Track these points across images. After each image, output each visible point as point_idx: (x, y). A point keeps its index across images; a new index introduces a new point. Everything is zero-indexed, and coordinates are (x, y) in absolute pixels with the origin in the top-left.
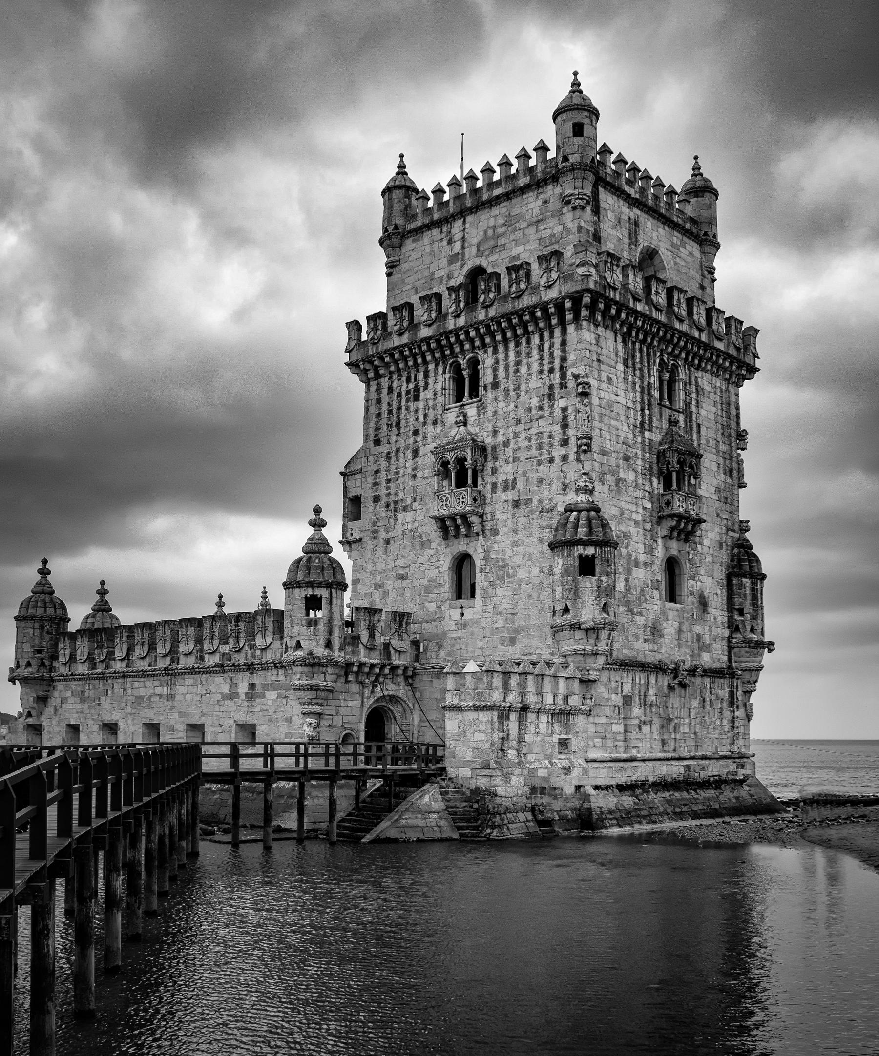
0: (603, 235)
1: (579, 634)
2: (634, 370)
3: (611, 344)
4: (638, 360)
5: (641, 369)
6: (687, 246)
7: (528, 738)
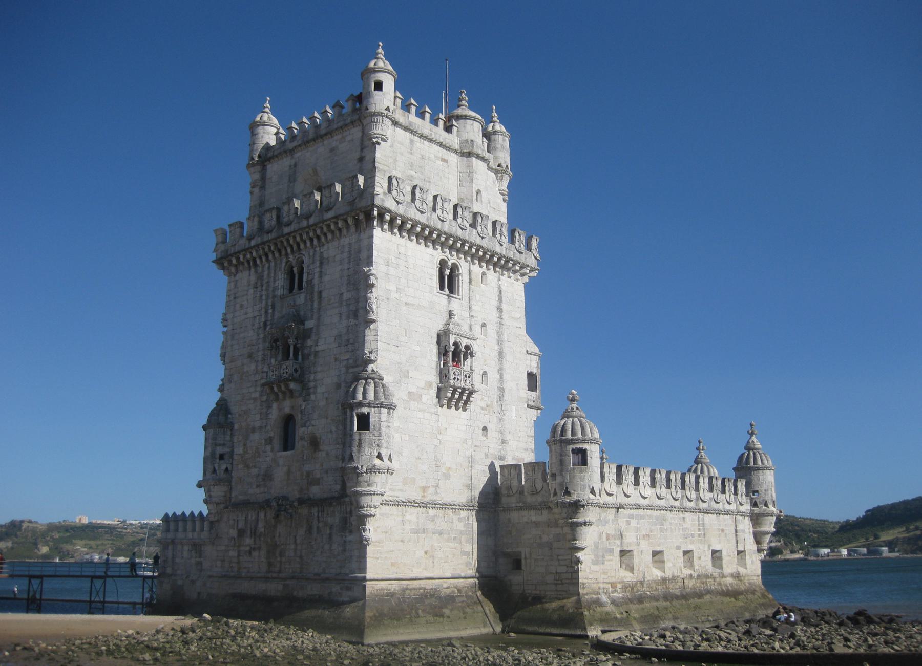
2: (262, 286)
4: (265, 277)
5: (268, 282)
6: (349, 138)
7: (178, 560)
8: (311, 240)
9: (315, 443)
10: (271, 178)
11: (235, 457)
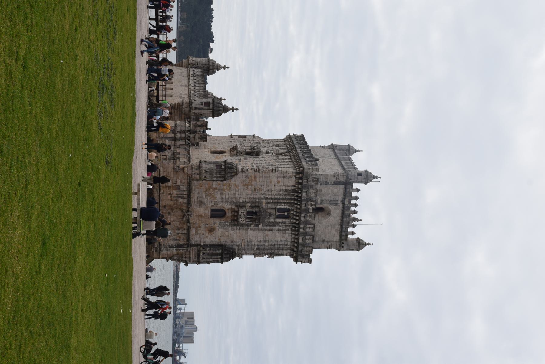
0: (328, 186)
1: (198, 164)
2: (285, 195)
3: (291, 183)
5: (285, 199)
6: (336, 233)
8: (295, 227)
9: (211, 230)
10: (337, 188)
11: (212, 182)
